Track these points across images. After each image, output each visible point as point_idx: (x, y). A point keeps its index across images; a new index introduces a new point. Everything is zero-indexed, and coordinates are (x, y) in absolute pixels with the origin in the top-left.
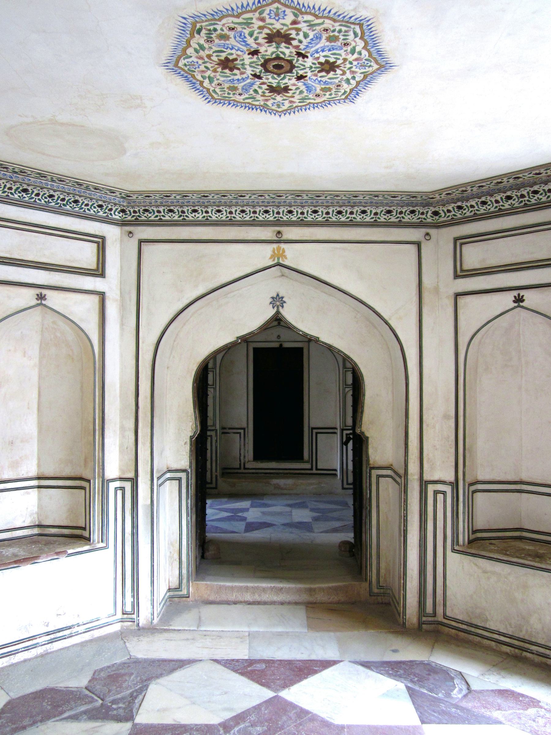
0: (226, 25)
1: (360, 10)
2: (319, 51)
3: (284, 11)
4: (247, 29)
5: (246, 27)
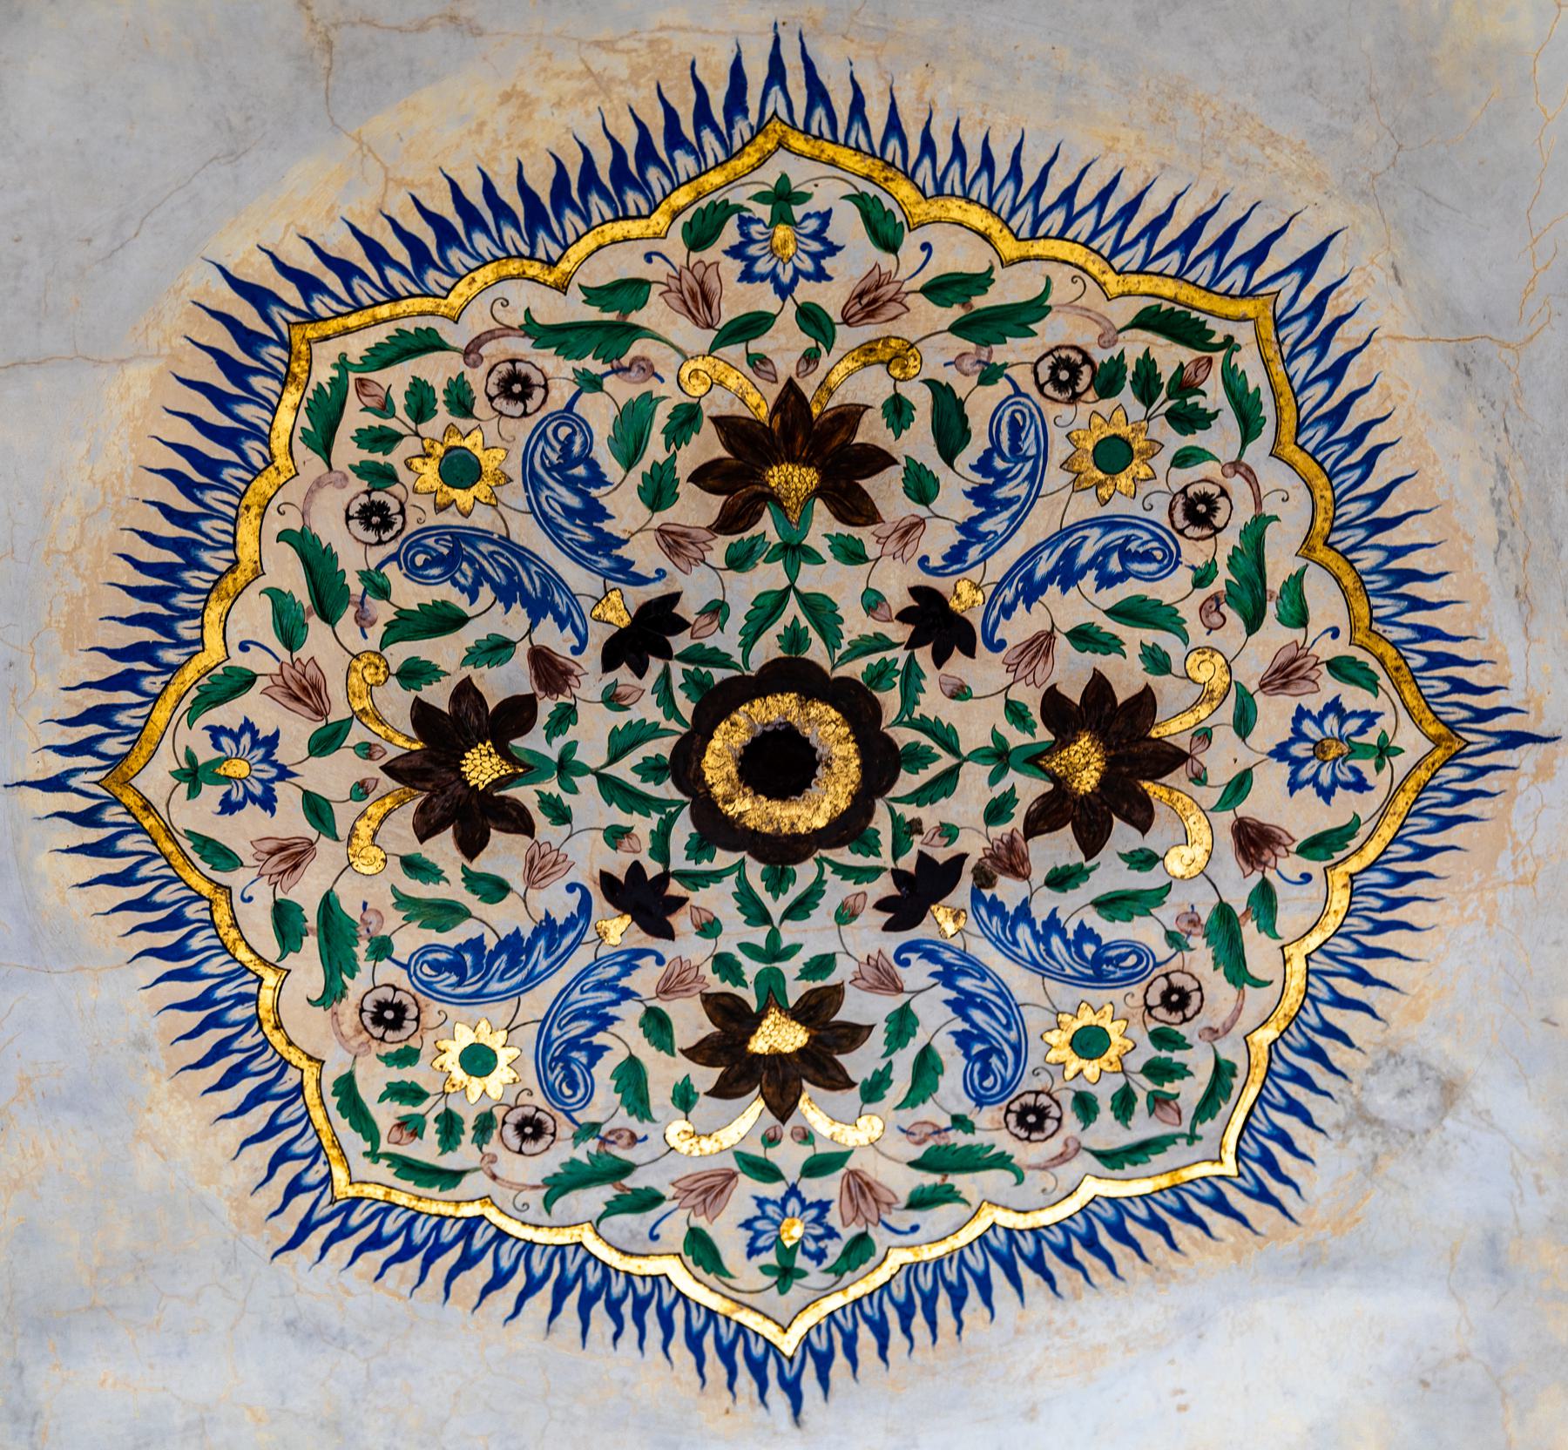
0: (1237, 485)
1: (1357, 1144)
2: (966, 983)
3: (1360, 785)
4: (1202, 595)
5: (1218, 585)
